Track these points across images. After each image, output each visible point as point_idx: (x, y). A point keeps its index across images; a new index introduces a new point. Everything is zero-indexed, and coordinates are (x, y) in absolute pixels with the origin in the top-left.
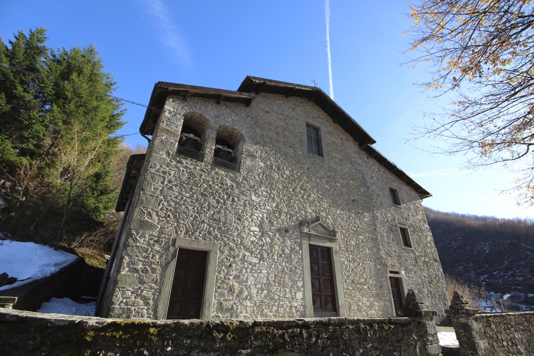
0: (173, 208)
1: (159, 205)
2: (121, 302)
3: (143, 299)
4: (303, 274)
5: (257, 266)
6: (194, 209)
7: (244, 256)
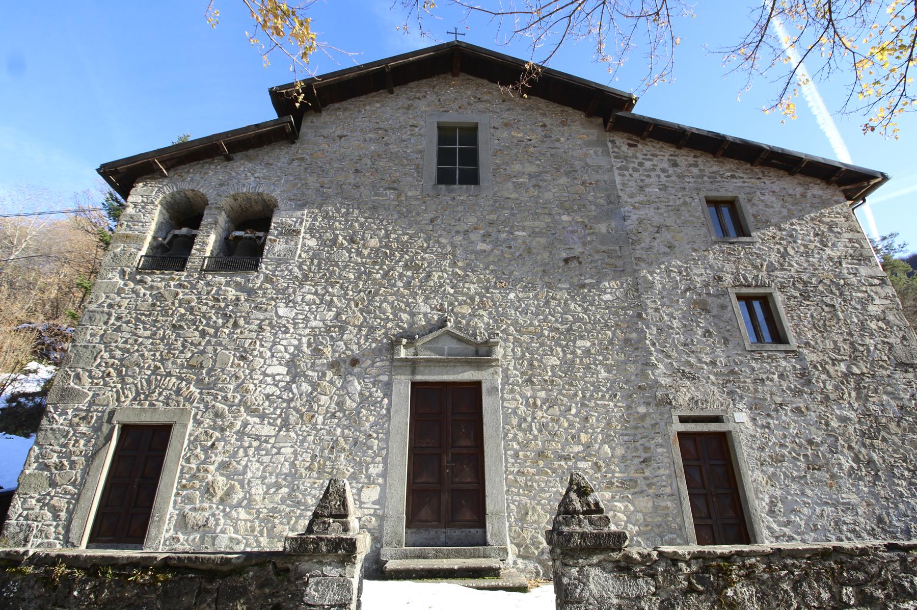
0: (118, 359)
1: (95, 360)
2: (20, 515)
3: (52, 510)
4: (387, 448)
5: (272, 441)
6: (154, 355)
7: (245, 424)
